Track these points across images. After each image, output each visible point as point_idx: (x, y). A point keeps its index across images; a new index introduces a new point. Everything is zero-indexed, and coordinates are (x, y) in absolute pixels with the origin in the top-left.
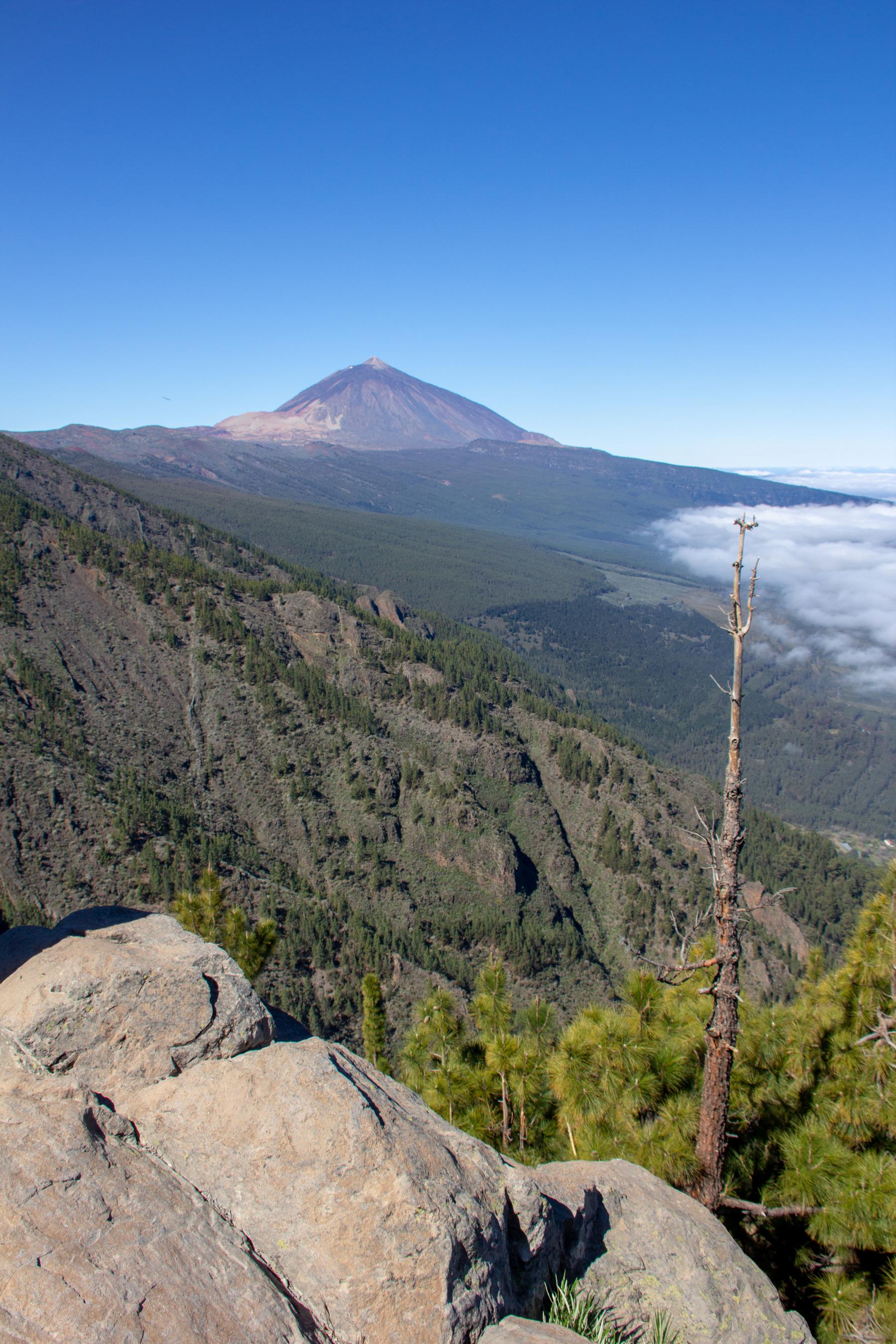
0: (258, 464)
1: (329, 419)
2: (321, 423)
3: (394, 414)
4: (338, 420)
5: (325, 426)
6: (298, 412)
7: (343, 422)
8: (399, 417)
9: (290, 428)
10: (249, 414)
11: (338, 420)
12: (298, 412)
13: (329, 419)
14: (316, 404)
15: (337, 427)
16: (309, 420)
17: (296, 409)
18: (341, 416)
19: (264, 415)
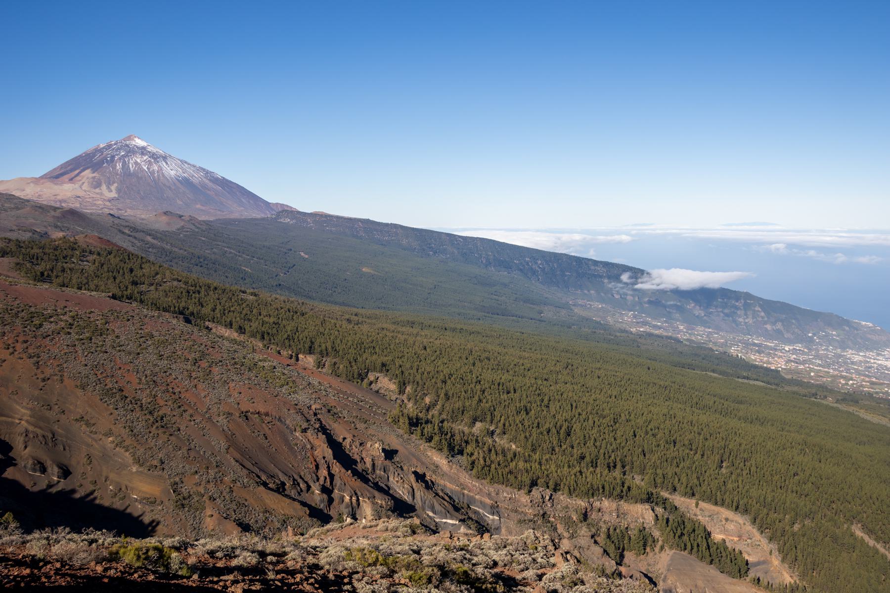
0: (149, 238)
1: (104, 187)
2: (97, 190)
3: (164, 185)
4: (113, 188)
5: (102, 194)
6: (71, 180)
7: (119, 191)
8: (170, 188)
9: (69, 194)
10: (22, 179)
11: (113, 188)
12: (71, 180)
13: (104, 187)
14: (88, 173)
15: (114, 195)
16: (85, 187)
17: (66, 178)
18: (116, 185)
19: (36, 181)
